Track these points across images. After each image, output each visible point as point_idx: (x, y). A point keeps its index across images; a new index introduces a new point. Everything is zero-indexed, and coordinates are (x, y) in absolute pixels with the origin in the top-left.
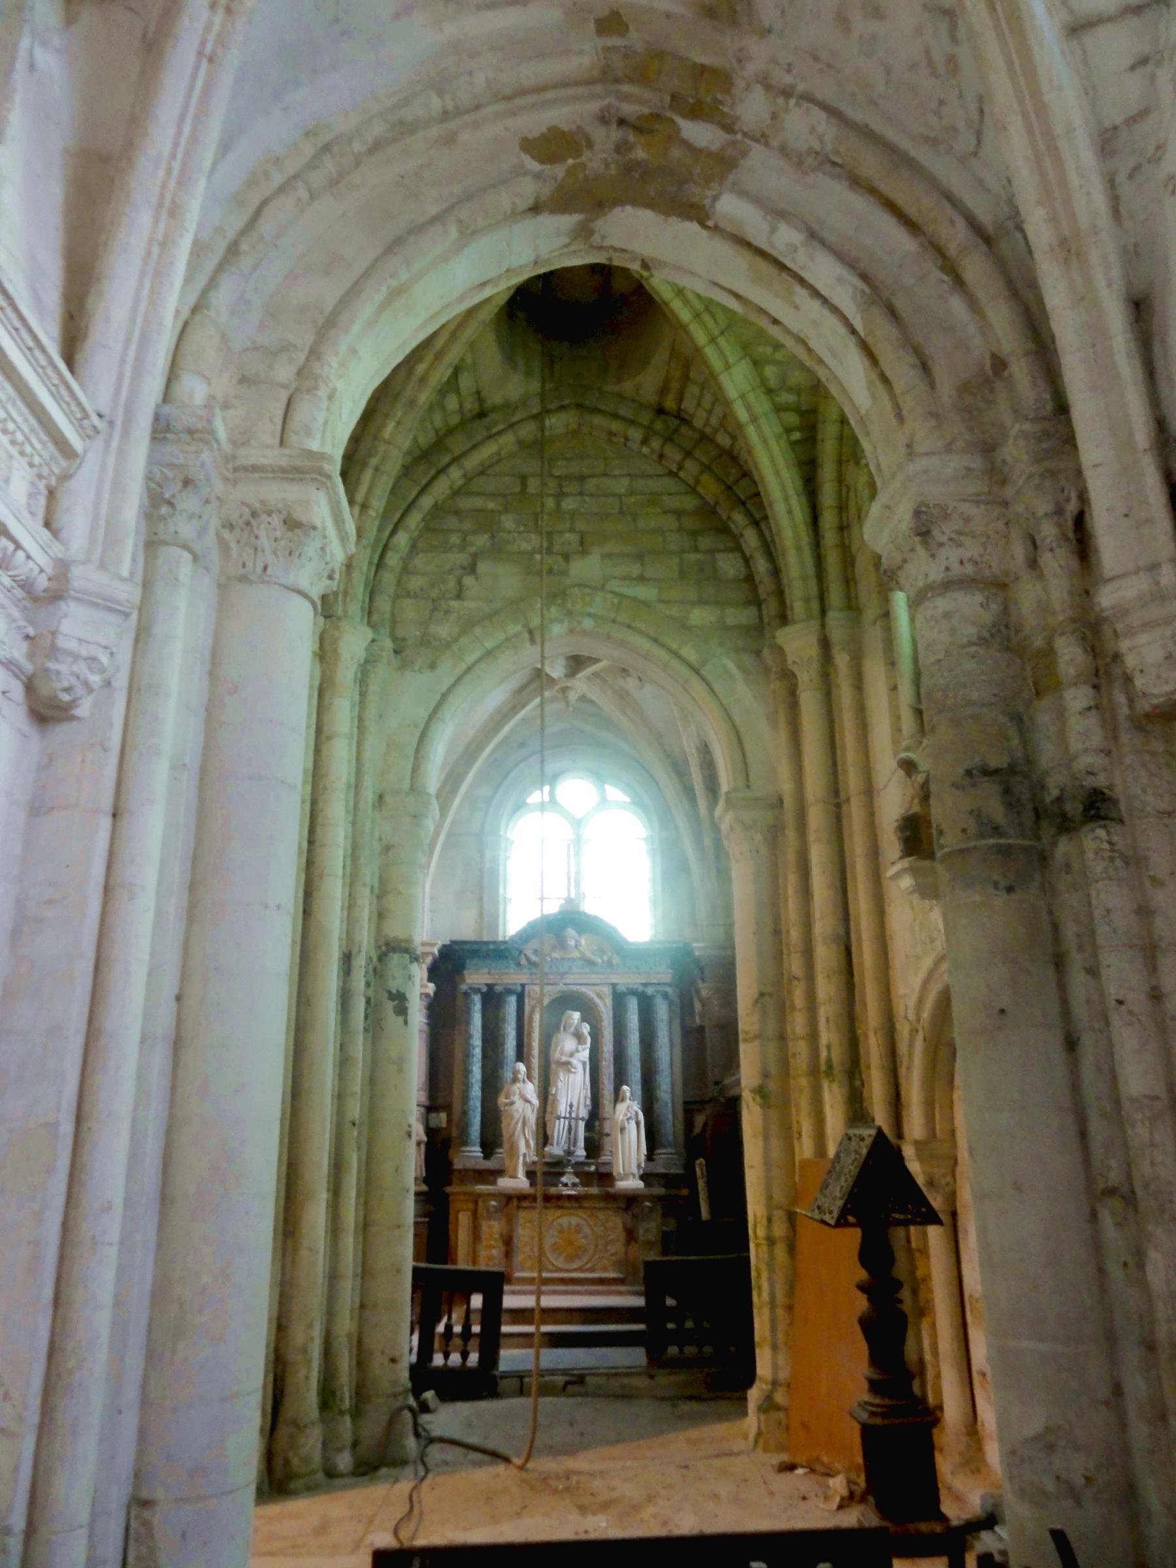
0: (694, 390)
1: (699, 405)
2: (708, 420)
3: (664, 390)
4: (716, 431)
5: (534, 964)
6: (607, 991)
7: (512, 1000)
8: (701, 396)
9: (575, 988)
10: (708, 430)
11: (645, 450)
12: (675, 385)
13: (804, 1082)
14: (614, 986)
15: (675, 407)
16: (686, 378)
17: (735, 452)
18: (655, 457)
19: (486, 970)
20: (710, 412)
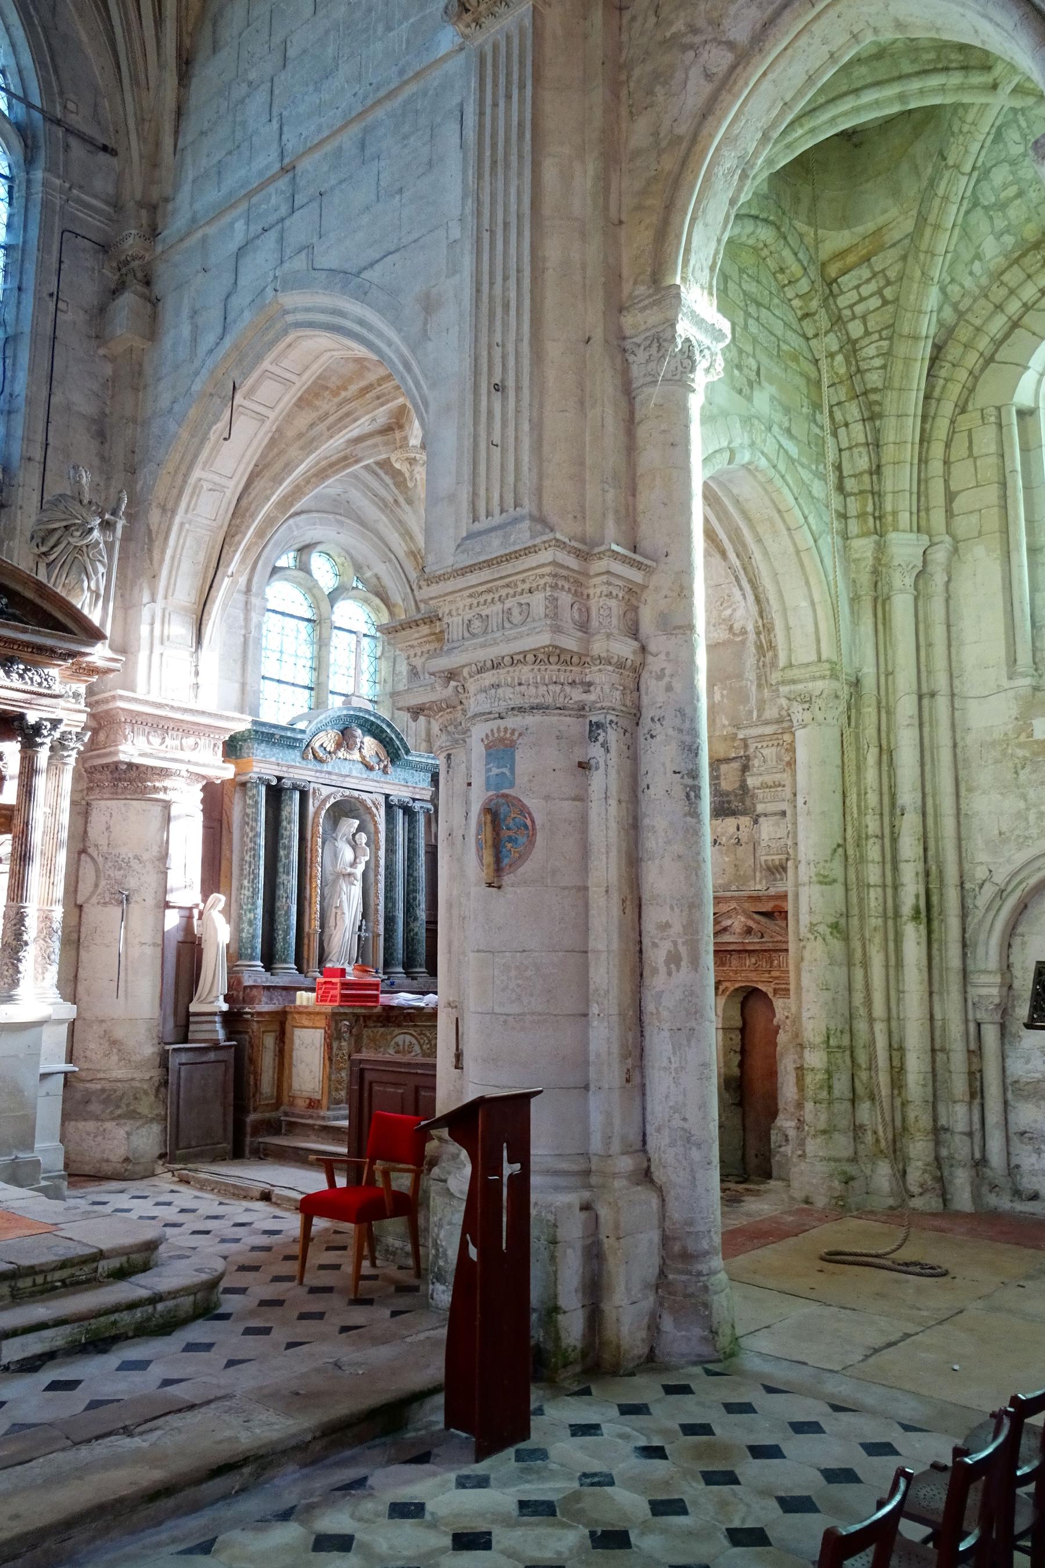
0: (866, 273)
1: (857, 287)
2: (855, 304)
3: (840, 255)
4: (854, 317)
5: (321, 761)
6: (382, 800)
7: (297, 795)
8: (868, 281)
9: (356, 794)
10: (847, 313)
11: (796, 303)
12: (851, 259)
13: (875, 922)
14: (387, 796)
15: (833, 275)
16: (867, 259)
17: (857, 347)
18: (800, 313)
19: (273, 759)
20: (862, 299)
